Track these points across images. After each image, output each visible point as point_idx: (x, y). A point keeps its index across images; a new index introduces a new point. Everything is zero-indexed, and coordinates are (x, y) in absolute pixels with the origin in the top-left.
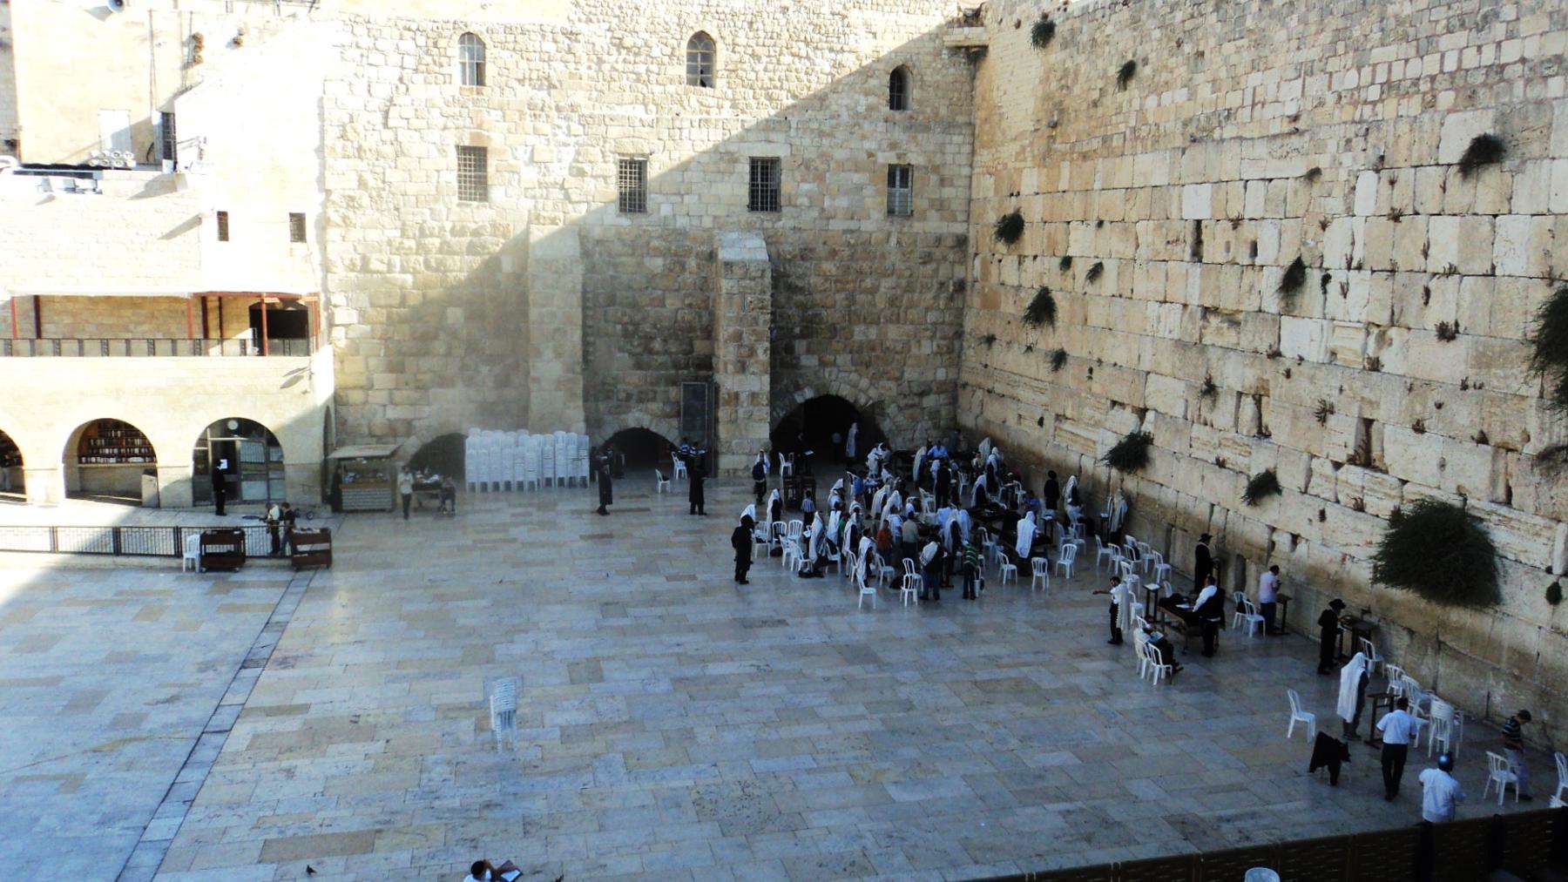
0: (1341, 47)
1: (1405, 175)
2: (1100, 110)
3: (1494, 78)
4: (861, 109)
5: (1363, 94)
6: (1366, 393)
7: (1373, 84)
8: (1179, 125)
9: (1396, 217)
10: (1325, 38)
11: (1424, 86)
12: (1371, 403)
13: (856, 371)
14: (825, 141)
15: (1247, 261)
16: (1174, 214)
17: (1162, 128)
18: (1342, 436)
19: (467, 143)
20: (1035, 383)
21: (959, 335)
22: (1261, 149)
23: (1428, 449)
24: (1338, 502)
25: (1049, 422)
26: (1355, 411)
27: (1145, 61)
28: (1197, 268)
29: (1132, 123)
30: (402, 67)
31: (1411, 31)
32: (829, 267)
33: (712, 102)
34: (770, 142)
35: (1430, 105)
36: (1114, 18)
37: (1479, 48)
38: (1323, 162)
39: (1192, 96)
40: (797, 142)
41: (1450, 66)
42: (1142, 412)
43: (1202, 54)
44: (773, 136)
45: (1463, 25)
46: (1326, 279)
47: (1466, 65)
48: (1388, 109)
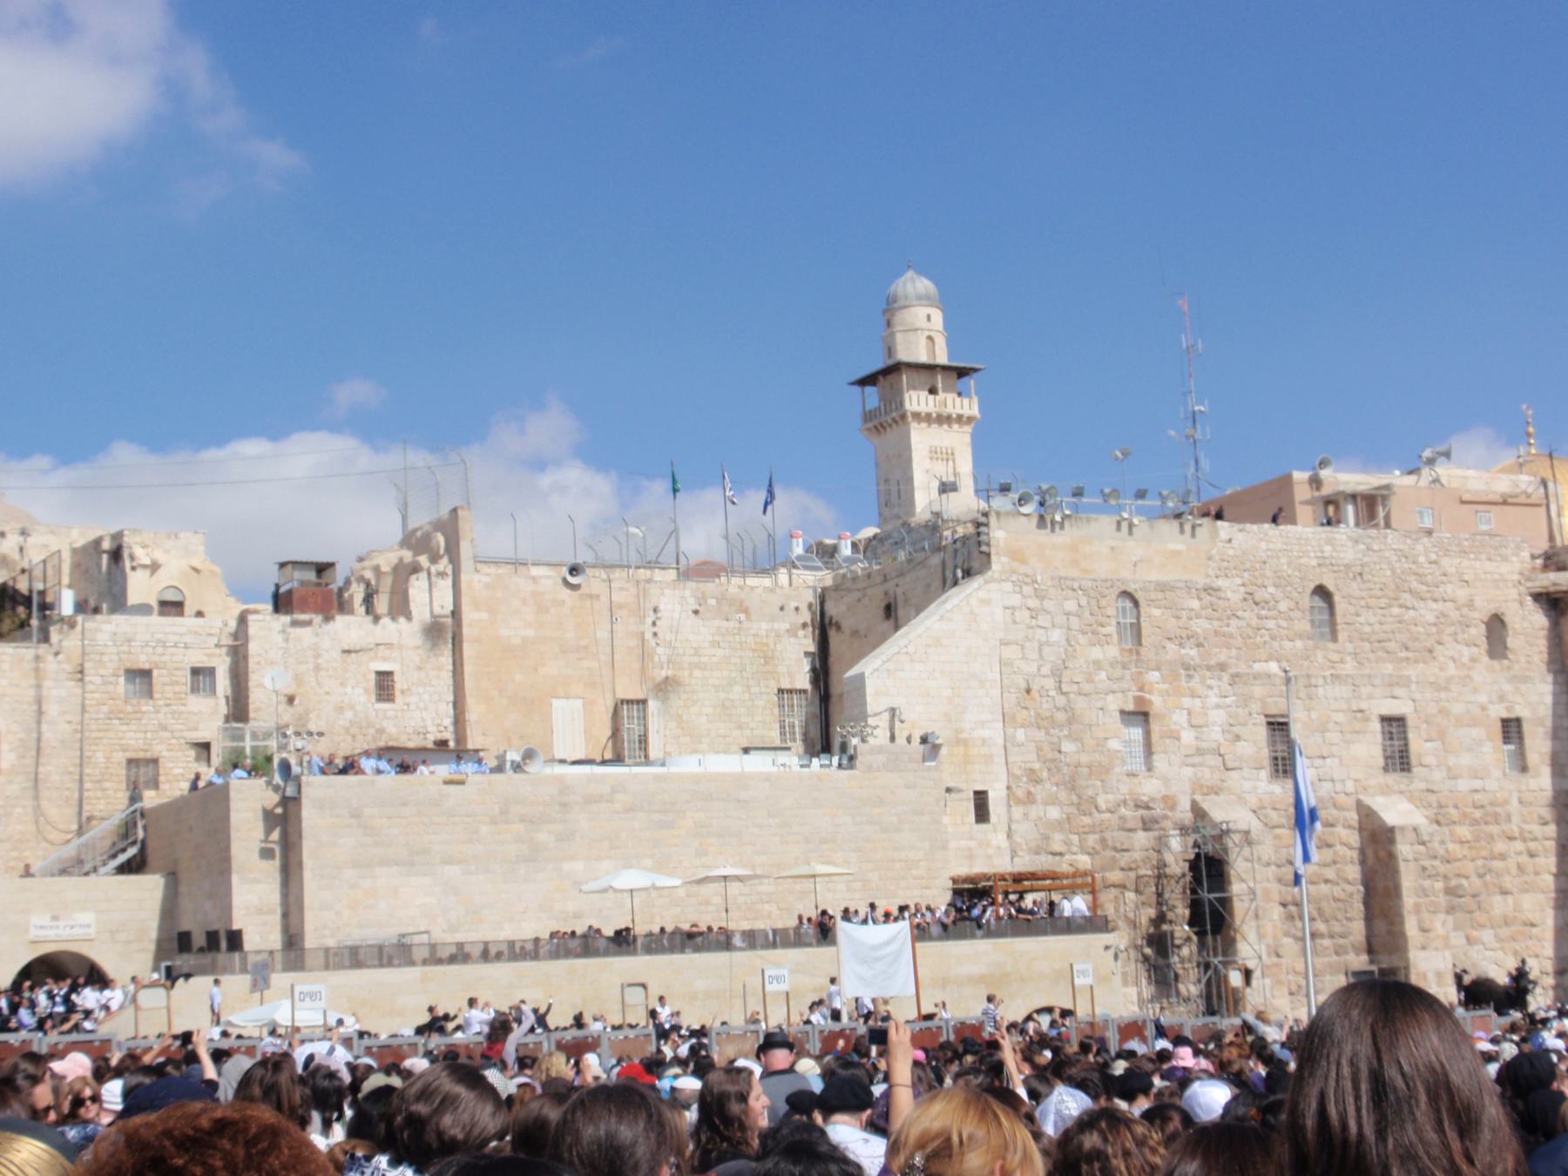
4: (1465, 660)
13: (1502, 949)
14: (1443, 695)
19: (1130, 707)
30: (1069, 629)
32: (1464, 831)
33: (1336, 657)
34: (1394, 697)
40: (1418, 696)
44: (1398, 691)
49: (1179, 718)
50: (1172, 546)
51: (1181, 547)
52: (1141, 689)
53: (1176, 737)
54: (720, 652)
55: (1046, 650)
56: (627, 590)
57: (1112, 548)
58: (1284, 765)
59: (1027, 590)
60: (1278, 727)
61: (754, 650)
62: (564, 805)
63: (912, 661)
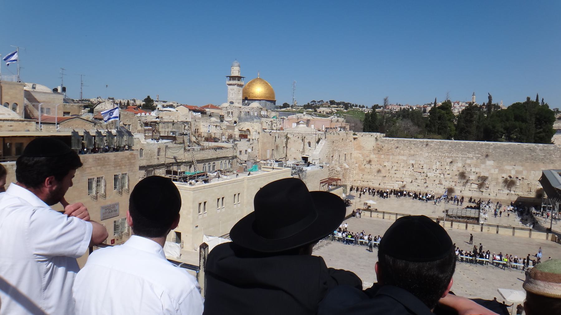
2: (390, 150)
9: (441, 165)
10: (431, 150)
15: (422, 168)
16: (408, 163)
17: (405, 154)
18: (437, 182)
22: (423, 158)
23: (448, 182)
25: (382, 184)
26: (439, 180)
27: (400, 147)
29: (398, 153)
35: (445, 158)
38: (432, 160)
39: (410, 152)
41: (447, 155)
42: (403, 182)
46: (433, 170)
48: (440, 157)
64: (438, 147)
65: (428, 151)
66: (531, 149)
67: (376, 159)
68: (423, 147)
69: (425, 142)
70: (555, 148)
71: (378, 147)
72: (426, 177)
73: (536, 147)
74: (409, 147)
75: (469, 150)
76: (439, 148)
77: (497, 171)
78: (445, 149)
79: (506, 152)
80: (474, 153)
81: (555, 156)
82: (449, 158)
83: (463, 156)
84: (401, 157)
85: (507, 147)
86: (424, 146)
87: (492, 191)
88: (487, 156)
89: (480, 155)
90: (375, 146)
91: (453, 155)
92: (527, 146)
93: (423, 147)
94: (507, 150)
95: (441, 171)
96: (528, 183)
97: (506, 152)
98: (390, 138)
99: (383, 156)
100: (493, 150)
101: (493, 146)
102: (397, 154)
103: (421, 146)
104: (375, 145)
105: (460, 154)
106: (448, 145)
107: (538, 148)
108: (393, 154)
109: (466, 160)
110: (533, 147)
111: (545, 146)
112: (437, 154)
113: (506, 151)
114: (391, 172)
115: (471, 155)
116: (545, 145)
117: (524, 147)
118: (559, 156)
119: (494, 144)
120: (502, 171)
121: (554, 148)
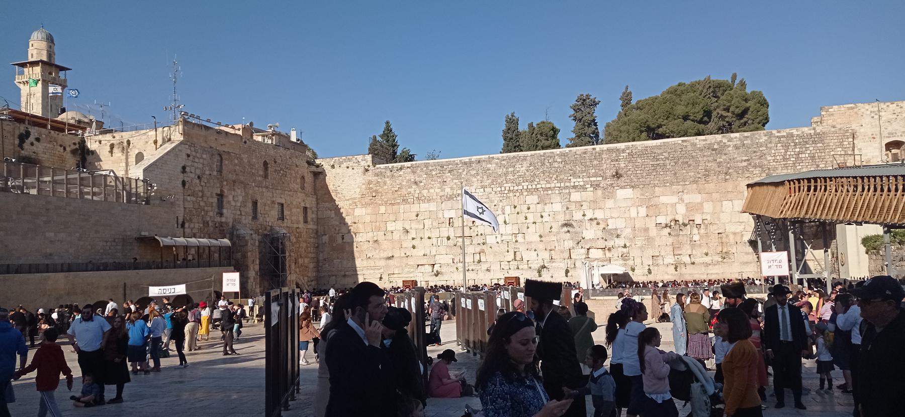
0: (495, 183)
1: (518, 206)
2: (399, 193)
3: (536, 190)
5: (503, 192)
6: (515, 247)
7: (505, 190)
8: (439, 197)
11: (519, 191)
12: (517, 248)
16: (441, 216)
17: (431, 198)
20: (375, 268)
21: (318, 262)
24: (510, 269)
25: (385, 277)
28: (452, 229)
31: (514, 182)
36: (403, 171)
37: (532, 186)
39: (443, 190)
40: (286, 198)
41: (525, 187)
43: (446, 182)
45: (527, 181)
47: (529, 188)
48: (511, 194)
49: (231, 198)
50: (231, 141)
51: (233, 142)
52: (222, 187)
53: (229, 202)
54: (46, 156)
55: (197, 170)
56: (10, 125)
57: (216, 139)
58: (255, 218)
59: (193, 149)
60: (255, 204)
61: (58, 157)
62: (48, 210)
63: (157, 168)
64: (505, 170)
65: (483, 184)
66: (715, 147)
67: (368, 219)
68: (471, 175)
69: (473, 162)
70: (770, 137)
71: (370, 188)
72: (484, 247)
73: (725, 141)
74: (439, 180)
75: (575, 169)
76: (506, 174)
77: (643, 211)
78: (520, 174)
79: (658, 162)
80: (585, 174)
81: (773, 158)
82: (530, 192)
83: (562, 185)
84: (424, 206)
85: (659, 151)
86: (474, 172)
87: (638, 261)
88: (618, 175)
89: (601, 179)
90: (364, 186)
91: (539, 186)
92: (704, 143)
93: (471, 175)
94: (661, 157)
95: (516, 227)
96: (720, 232)
97: (658, 162)
98: (395, 165)
99: (382, 209)
100: (629, 162)
101: (627, 151)
102: (415, 198)
103: (465, 173)
104: (363, 184)
105: (556, 181)
106: (526, 164)
107: (729, 143)
108: (405, 201)
109: (570, 194)
110: (718, 143)
111: (747, 137)
112: (503, 189)
113: (658, 160)
114: (404, 245)
115: (579, 182)
116: (746, 134)
117: (698, 146)
118: (781, 157)
119: (628, 148)
120: (653, 209)
121: (766, 138)
